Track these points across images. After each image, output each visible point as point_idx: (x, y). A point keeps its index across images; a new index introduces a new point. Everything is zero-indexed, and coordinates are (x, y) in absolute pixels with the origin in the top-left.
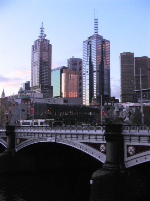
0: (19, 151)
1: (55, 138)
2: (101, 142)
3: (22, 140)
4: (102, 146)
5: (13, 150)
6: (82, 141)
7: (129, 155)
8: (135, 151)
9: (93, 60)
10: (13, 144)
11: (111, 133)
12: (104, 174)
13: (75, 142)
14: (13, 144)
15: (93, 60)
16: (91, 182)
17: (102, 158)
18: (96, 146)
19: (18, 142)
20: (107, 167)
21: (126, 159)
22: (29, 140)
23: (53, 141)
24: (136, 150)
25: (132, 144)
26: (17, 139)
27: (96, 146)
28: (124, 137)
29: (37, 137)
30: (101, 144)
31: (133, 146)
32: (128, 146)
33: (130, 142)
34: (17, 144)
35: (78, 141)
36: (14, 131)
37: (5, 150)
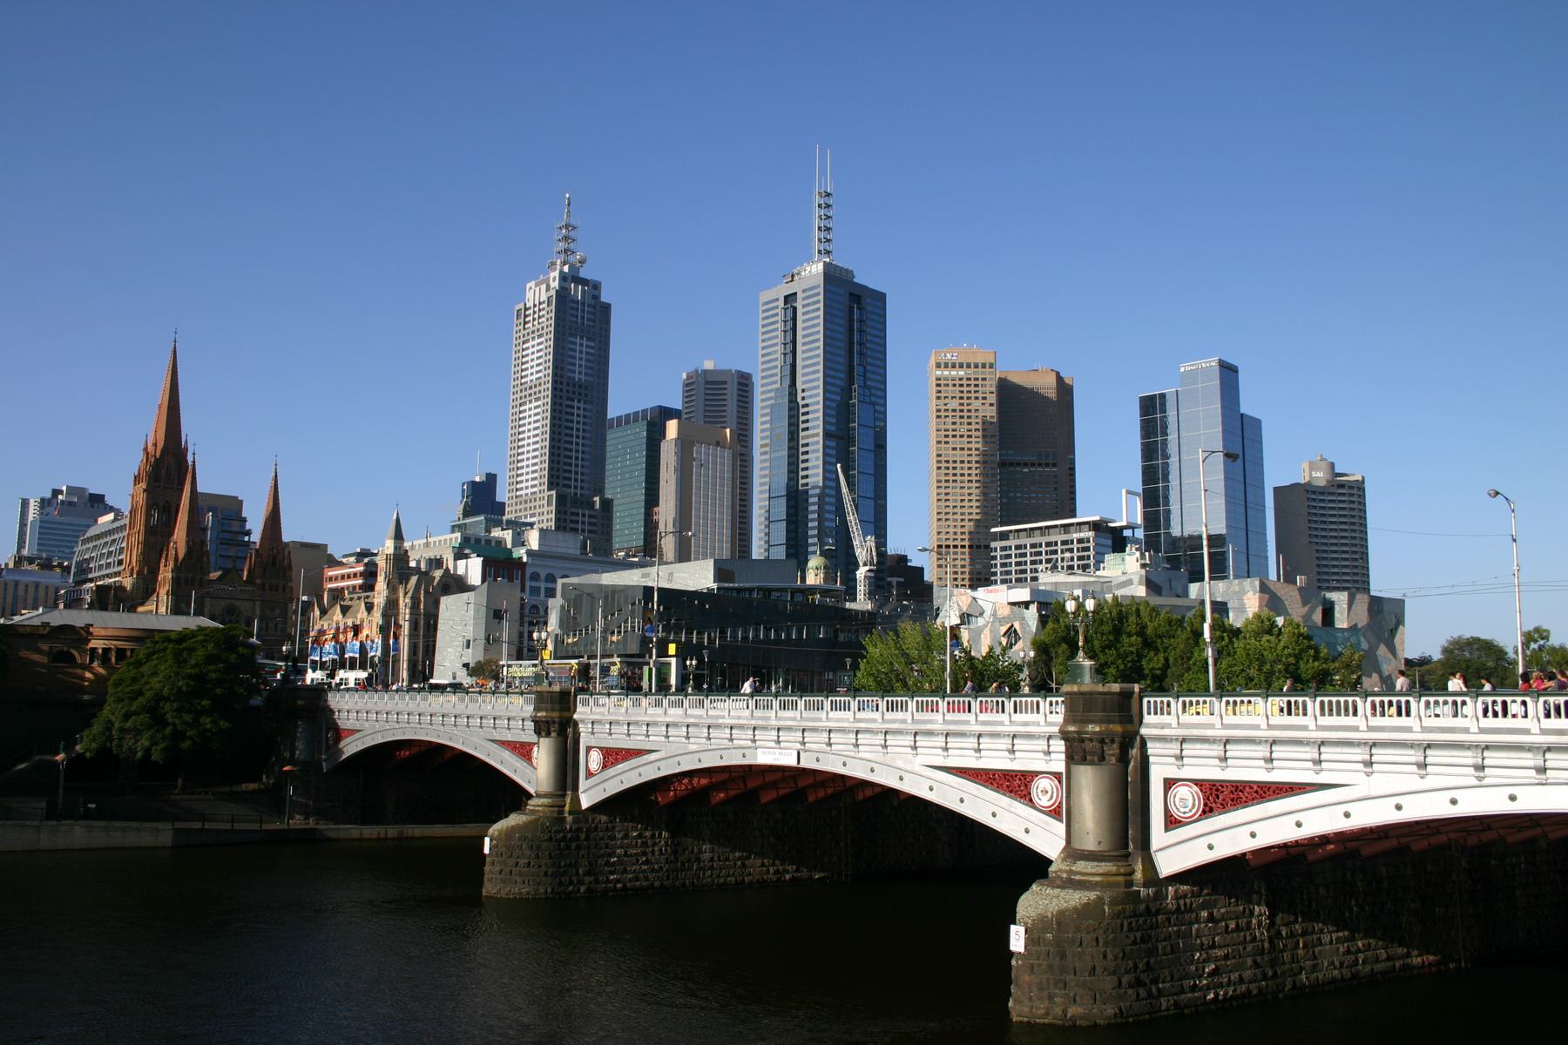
0: (596, 808)
1: (799, 746)
3: (613, 756)
4: (1043, 783)
5: (568, 800)
6: (940, 762)
7: (1172, 822)
8: (1205, 805)
10: (567, 770)
11: (1098, 729)
12: (1073, 903)
13: (900, 764)
14: (567, 770)
16: (1017, 940)
17: (1046, 838)
18: (1015, 784)
19: (594, 766)
20: (1077, 873)
23: (789, 760)
24: (1207, 798)
26: (589, 749)
27: (1015, 784)
30: (1036, 774)
31: (1198, 783)
32: (1169, 784)
33: (1179, 767)
34: (589, 774)
35: (920, 760)
36: (575, 716)
37: (530, 802)
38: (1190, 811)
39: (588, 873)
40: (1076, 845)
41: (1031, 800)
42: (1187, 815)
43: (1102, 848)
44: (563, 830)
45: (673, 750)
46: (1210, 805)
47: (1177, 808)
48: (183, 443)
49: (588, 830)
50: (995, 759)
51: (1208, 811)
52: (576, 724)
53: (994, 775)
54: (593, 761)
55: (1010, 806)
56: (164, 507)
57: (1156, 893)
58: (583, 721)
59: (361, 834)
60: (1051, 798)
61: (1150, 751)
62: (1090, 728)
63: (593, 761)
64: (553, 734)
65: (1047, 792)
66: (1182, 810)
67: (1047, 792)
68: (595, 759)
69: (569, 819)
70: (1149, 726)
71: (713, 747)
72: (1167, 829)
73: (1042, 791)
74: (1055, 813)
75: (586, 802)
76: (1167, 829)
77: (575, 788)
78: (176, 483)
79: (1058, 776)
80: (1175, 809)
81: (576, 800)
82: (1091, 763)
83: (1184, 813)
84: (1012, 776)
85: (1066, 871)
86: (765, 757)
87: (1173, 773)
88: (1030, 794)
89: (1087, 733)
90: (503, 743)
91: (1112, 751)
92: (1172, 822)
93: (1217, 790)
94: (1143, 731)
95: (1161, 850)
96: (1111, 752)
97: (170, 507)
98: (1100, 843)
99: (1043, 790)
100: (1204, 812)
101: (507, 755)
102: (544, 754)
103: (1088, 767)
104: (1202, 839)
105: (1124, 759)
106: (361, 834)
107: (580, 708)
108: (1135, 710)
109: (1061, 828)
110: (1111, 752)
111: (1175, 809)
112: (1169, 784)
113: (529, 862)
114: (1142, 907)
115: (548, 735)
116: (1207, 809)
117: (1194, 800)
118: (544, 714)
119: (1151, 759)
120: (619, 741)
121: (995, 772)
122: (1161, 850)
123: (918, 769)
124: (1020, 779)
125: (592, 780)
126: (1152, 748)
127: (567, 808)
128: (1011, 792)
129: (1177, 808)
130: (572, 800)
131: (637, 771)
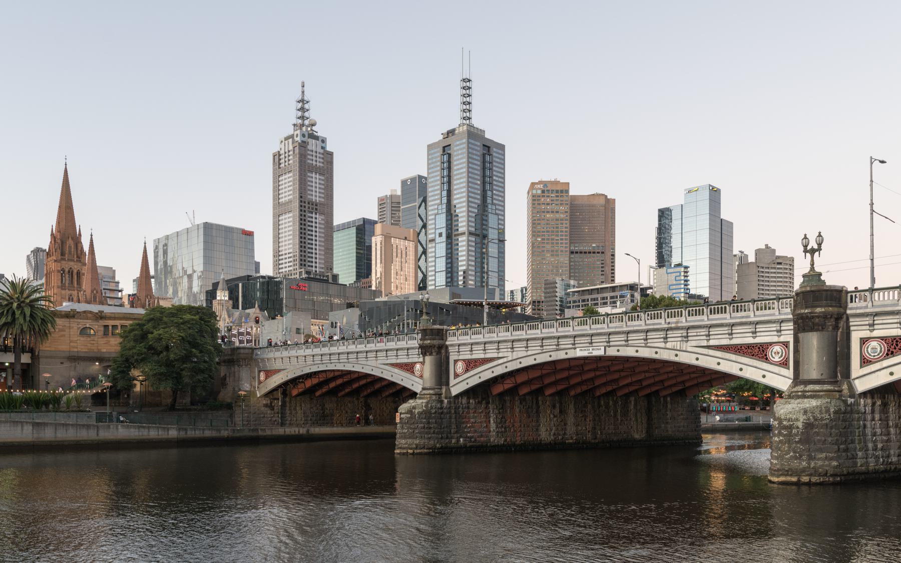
1: (605, 344)
2: (775, 339)
3: (471, 364)
6: (705, 343)
7: (865, 362)
8: (889, 350)
9: (476, 201)
15: (476, 201)
17: (781, 380)
18: (759, 352)
21: (856, 369)
22: (501, 361)
23: (600, 352)
25: (876, 333)
26: (456, 361)
28: (851, 320)
29: (535, 348)
30: (771, 344)
31: (882, 338)
32: (864, 341)
33: (871, 331)
34: (456, 376)
35: (689, 344)
36: (447, 343)
38: (878, 355)
39: (456, 432)
40: (804, 376)
41: (767, 359)
42: (876, 357)
43: (823, 377)
44: (442, 408)
45: (515, 355)
46: (891, 350)
47: (869, 354)
48: (78, 231)
49: (455, 408)
50: (743, 338)
51: (890, 354)
52: (447, 347)
53: (741, 347)
54: (459, 368)
55: (741, 369)
56: (69, 272)
57: (854, 402)
58: (452, 345)
59: (285, 431)
60: (781, 356)
61: (851, 324)
62: (818, 310)
63: (459, 368)
64: (434, 354)
65: (778, 353)
66: (873, 355)
67: (778, 353)
68: (460, 367)
69: (446, 401)
70: (851, 309)
71: (544, 351)
72: (861, 367)
73: (775, 353)
74: (784, 364)
75: (455, 391)
76: (861, 367)
77: (447, 384)
78: (75, 256)
79: (786, 344)
80: (868, 355)
81: (448, 391)
82: (817, 330)
83: (874, 356)
84: (753, 347)
85: (801, 392)
86: (579, 353)
87: (866, 334)
88: (766, 355)
89: (816, 313)
90: (392, 365)
91: (830, 323)
92: (865, 362)
93: (897, 341)
94: (849, 312)
95: (857, 378)
96: (830, 324)
97: (72, 272)
98: (822, 374)
99: (776, 354)
100: (887, 354)
101: (396, 370)
102: (426, 368)
103: (815, 333)
104: (885, 370)
105: (836, 328)
106: (285, 431)
107: (449, 339)
108: (843, 301)
109: (790, 373)
110: (830, 324)
111: (868, 355)
112: (864, 341)
113: (424, 426)
114: (849, 408)
115: (431, 354)
116: (890, 353)
117: (881, 349)
118: (429, 342)
119: (852, 328)
120: (478, 355)
121: (741, 345)
122: (857, 378)
123: (689, 349)
124: (759, 348)
125: (460, 379)
126: (853, 322)
127: (443, 396)
128: (753, 355)
129: (869, 354)
130: (446, 390)
131: (478, 376)
